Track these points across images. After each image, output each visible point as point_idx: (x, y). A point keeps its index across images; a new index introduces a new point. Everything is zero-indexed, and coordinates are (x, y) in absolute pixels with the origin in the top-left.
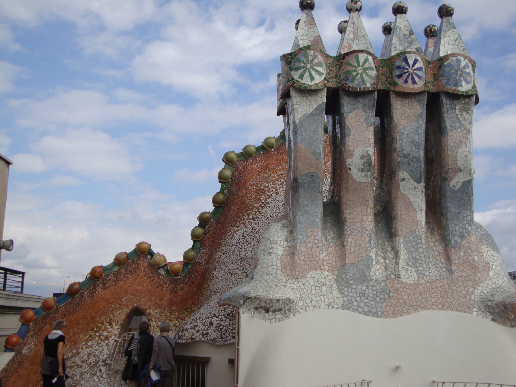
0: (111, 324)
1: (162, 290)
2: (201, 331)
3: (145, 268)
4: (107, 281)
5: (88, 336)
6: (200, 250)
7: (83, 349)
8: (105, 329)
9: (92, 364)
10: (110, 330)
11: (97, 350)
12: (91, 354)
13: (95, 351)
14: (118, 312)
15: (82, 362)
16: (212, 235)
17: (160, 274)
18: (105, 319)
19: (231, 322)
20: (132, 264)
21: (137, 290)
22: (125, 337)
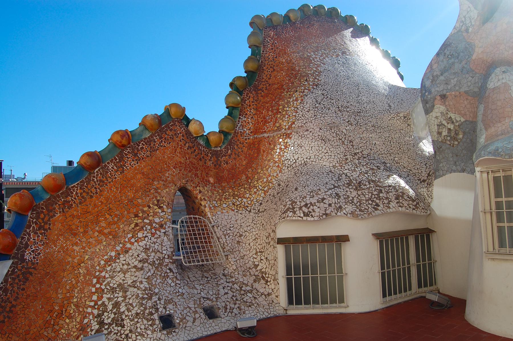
0: (160, 208)
1: (205, 163)
2: (333, 205)
3: (183, 136)
4: (138, 150)
5: (133, 226)
6: (240, 118)
7: (132, 244)
8: (155, 214)
9: (157, 262)
10: (161, 214)
11: (154, 243)
12: (149, 249)
13: (153, 245)
14: (165, 191)
15: (140, 261)
16: (253, 102)
17: (199, 144)
18: (150, 200)
19: (359, 193)
20: (167, 130)
21: (181, 163)
22: (182, 222)
